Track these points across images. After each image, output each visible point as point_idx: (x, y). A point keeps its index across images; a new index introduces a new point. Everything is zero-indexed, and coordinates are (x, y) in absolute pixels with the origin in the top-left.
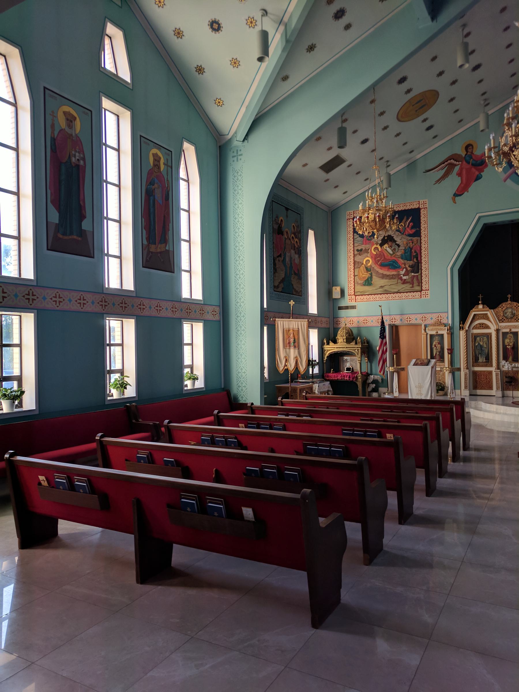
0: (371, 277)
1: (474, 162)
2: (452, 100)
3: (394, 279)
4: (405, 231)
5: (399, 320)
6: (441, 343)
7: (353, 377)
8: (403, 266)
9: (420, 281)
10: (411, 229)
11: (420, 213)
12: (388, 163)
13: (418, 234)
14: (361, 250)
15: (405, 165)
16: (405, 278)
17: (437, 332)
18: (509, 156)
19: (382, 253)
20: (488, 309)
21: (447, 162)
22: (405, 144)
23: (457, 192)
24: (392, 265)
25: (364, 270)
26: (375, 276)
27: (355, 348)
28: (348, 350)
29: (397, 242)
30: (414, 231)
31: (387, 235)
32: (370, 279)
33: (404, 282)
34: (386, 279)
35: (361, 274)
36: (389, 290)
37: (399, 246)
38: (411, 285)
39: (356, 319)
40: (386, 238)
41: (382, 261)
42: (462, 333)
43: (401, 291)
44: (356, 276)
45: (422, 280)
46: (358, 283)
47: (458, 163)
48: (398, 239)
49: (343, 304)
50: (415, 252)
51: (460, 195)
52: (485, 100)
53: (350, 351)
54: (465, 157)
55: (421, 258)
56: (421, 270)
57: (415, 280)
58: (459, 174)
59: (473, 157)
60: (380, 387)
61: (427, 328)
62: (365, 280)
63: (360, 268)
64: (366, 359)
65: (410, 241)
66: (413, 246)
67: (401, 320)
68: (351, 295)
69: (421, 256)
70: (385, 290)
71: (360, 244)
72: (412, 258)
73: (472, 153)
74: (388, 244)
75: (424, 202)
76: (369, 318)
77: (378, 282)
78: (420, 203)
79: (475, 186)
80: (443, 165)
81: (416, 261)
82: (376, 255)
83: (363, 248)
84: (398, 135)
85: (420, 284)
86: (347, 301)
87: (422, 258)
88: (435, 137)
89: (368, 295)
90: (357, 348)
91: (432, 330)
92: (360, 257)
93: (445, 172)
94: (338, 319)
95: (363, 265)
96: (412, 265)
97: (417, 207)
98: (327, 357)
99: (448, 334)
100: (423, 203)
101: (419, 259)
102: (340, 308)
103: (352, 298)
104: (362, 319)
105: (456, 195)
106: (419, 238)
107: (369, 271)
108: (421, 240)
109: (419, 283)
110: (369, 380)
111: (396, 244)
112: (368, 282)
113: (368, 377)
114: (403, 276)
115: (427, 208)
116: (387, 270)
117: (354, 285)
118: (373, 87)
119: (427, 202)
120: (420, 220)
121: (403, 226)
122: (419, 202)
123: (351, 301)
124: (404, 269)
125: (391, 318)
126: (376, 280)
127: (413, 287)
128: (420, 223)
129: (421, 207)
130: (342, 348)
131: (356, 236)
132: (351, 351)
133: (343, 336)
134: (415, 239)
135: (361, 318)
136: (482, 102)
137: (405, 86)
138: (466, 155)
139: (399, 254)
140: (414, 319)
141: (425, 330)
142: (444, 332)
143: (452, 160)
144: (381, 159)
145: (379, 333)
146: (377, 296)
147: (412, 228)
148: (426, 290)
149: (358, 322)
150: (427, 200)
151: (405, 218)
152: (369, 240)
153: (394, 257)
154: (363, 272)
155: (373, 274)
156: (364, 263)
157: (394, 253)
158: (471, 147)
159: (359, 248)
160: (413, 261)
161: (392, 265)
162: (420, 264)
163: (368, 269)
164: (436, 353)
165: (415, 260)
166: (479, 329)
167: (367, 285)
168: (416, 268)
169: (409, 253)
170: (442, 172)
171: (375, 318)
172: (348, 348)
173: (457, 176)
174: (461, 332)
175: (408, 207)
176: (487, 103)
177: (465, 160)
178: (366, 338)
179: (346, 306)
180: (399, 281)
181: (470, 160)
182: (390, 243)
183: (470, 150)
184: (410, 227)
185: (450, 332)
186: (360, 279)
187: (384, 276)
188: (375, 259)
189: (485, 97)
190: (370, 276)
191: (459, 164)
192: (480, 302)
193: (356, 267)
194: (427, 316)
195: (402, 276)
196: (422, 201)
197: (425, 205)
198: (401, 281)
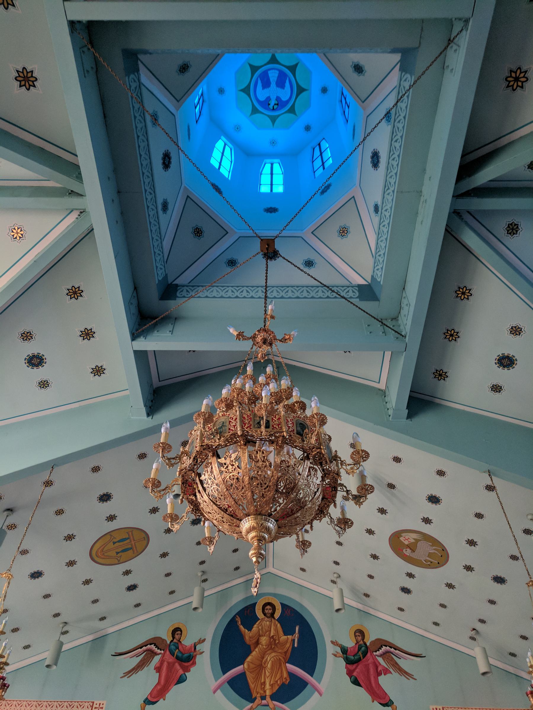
1: (180, 655)
2: (164, 555)
12: (65, 626)
15: (90, 638)
18: (196, 496)
21: (146, 646)
22: (95, 601)
23: (149, 698)
47: (159, 651)
51: (154, 703)
52: (204, 572)
54: (169, 645)
58: (158, 669)
59: (180, 647)
73: (179, 641)
78: (95, 706)
79: (175, 690)
80: (140, 650)
84: (87, 582)
88: (138, 605)
93: (141, 661)
100: (97, 706)
118: (53, 465)
119: (104, 706)
122: (93, 702)
136: (200, 574)
137: (107, 508)
138: (172, 641)
143: (153, 646)
144: (57, 615)
150: (105, 702)
158: (179, 632)
170: (136, 661)
173: (155, 671)
176: (204, 577)
177: (169, 650)
181: (175, 651)
183: (177, 637)
189: (203, 567)
196: (98, 703)
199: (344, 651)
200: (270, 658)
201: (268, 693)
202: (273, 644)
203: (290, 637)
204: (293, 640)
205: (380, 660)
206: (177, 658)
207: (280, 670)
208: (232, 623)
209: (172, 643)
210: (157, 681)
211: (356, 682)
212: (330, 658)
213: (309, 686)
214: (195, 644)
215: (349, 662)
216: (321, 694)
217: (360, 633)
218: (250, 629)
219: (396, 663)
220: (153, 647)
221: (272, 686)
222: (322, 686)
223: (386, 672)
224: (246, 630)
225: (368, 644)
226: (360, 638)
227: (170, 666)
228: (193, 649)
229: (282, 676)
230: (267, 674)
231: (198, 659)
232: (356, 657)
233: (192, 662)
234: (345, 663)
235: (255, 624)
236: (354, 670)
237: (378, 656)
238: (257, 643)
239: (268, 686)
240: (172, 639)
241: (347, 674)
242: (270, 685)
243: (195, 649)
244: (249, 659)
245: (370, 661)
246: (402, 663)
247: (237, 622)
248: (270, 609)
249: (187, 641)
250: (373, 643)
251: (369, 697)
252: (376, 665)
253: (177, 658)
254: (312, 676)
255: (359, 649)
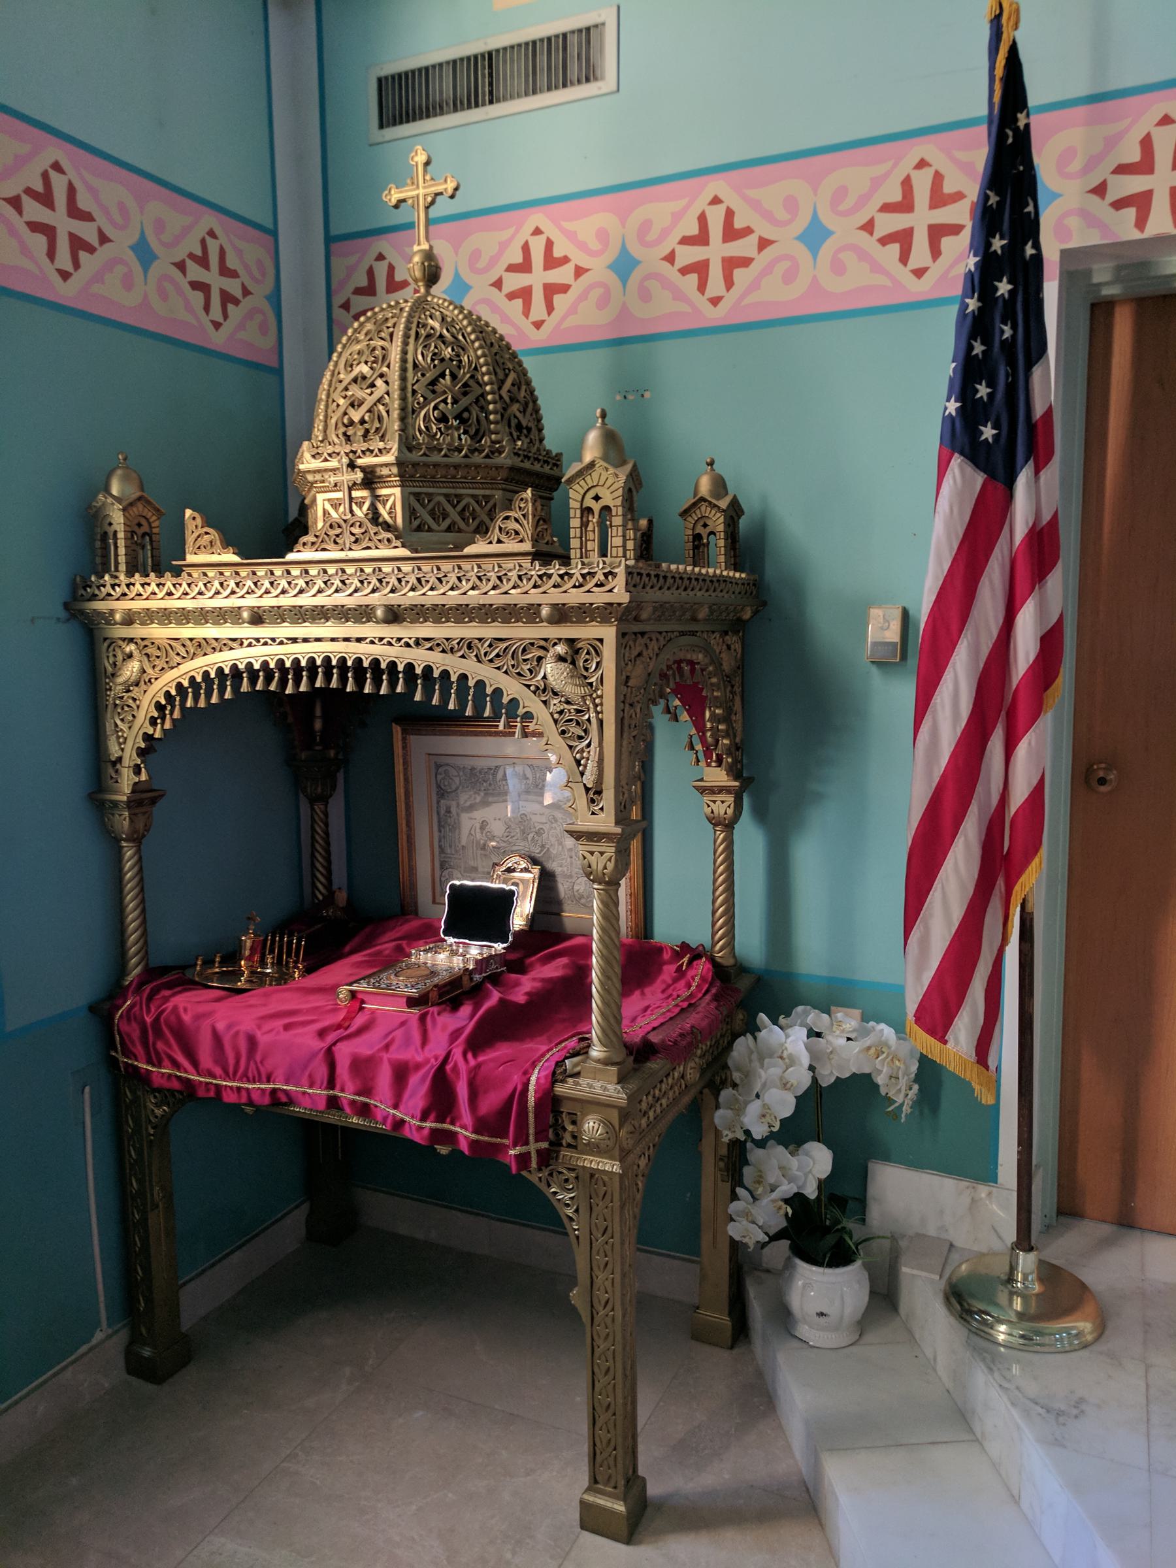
7: (490, 1102)
27: (530, 613)
28: (421, 658)
53: (455, 665)
60: (886, 1158)
64: (718, 776)
76: (772, 195)
90: (561, 614)
94: (382, 245)
110: (754, 1108)
113: (742, 1044)
125: (1111, 143)
130: (342, 614)
132: (476, 671)
133: (372, 429)
145: (946, 368)
149: (624, 266)
172: (420, 613)
178: (720, 486)
179: (473, 61)
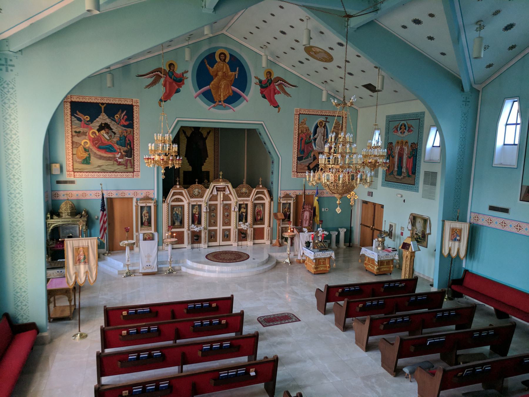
0: (89, 157)
1: (175, 78)
3: (111, 160)
4: (120, 122)
5: (115, 194)
6: (149, 212)
8: (118, 150)
9: (133, 164)
10: (125, 121)
11: (133, 109)
13: (131, 126)
14: (79, 132)
16: (120, 160)
17: (146, 205)
19: (99, 138)
20: (183, 188)
21: (155, 72)
24: (108, 149)
25: (82, 150)
26: (95, 157)
29: (113, 130)
30: (127, 123)
31: (104, 123)
32: (88, 159)
33: (120, 164)
34: (103, 160)
35: (79, 154)
36: (106, 169)
37: (115, 133)
38: (125, 167)
39: (74, 192)
40: (103, 125)
41: (99, 144)
42: (165, 206)
43: (116, 171)
44: (75, 154)
45: (134, 163)
46: (76, 161)
48: (114, 127)
49: (61, 179)
50: (129, 140)
51: (165, 101)
55: (133, 146)
56: (134, 155)
57: (129, 162)
58: (165, 85)
59: (175, 75)
61: (138, 202)
62: (84, 158)
63: (78, 148)
65: (124, 131)
66: (127, 135)
67: (117, 194)
68: (69, 171)
69: (134, 144)
70: (103, 169)
71: (78, 126)
72: (126, 145)
73: (173, 71)
74: (105, 130)
75: (138, 102)
77: (95, 161)
79: (175, 96)
80: (152, 74)
81: (129, 148)
82: (93, 138)
83: (81, 130)
85: (133, 166)
86: (66, 177)
87: (134, 146)
89: (87, 172)
91: (142, 203)
92: (78, 138)
95: (81, 146)
96: (126, 151)
97: (130, 104)
98: (52, 229)
99: (154, 206)
101: (132, 146)
102: (58, 182)
103: (71, 174)
104: (81, 193)
105: (161, 100)
106: (132, 130)
107: (87, 152)
108: (133, 131)
109: (132, 166)
111: (113, 132)
112: (87, 161)
114: (119, 159)
115: (138, 106)
116: (104, 152)
117: (73, 162)
120: (133, 115)
121: (119, 117)
123: (70, 177)
124: (120, 153)
126: (93, 160)
127: (127, 168)
128: (133, 117)
129: (134, 104)
131: (74, 119)
134: (129, 130)
135: (80, 192)
138: (169, 71)
139: (115, 140)
140: (127, 194)
141: (137, 203)
142: (152, 205)
146: (96, 174)
147: (126, 120)
148: (137, 172)
150: (139, 100)
151: (120, 111)
152: (87, 124)
153: (111, 142)
154: (81, 152)
155: (91, 155)
156: (83, 144)
157: (110, 139)
158: (173, 66)
159: (78, 130)
160: (127, 147)
161: (109, 149)
162: (133, 151)
163: (86, 150)
164: (145, 220)
165: (129, 147)
166: (176, 202)
167: (85, 164)
168: (130, 153)
169: (123, 141)
170: (151, 80)
171: (93, 192)
174: (164, 204)
175: (123, 102)
180: (115, 163)
182: (107, 130)
183: (171, 68)
184: (124, 119)
185: (156, 204)
186: (78, 158)
187: (101, 158)
188: (93, 142)
190: (88, 156)
191: (164, 77)
192: (177, 183)
193: (74, 146)
194: (138, 192)
195: (117, 158)
196: (135, 99)
197: (137, 103)
198: (116, 163)
199: (261, 82)
200: (223, 84)
201: (222, 99)
202: (225, 76)
203: (233, 73)
204: (236, 75)
205: (277, 87)
206: (174, 80)
207: (228, 90)
208: (202, 63)
209: (170, 72)
210: (164, 91)
211: (264, 97)
212: (253, 85)
213: (242, 97)
214: (182, 73)
215: (262, 87)
216: (247, 101)
217: (269, 73)
218: (212, 67)
219: (284, 89)
220: (159, 73)
221: (224, 96)
222: (248, 98)
223: (279, 93)
224: (211, 68)
225: (272, 79)
226: (269, 76)
227: (171, 84)
228: (182, 76)
229: (229, 93)
230: (222, 91)
231: (185, 81)
232: (266, 85)
233: (182, 82)
234: (260, 88)
235: (215, 64)
236: (264, 91)
237: (276, 85)
238: (217, 75)
239: (222, 96)
240: (169, 69)
241: (261, 93)
242: (223, 96)
243: (183, 76)
244: (212, 83)
245: (272, 88)
246: (286, 89)
247: (205, 63)
248: (223, 57)
249: (179, 71)
250: (275, 78)
251: (268, 103)
252: (275, 89)
253: (174, 80)
254: (244, 93)
255: (268, 82)
